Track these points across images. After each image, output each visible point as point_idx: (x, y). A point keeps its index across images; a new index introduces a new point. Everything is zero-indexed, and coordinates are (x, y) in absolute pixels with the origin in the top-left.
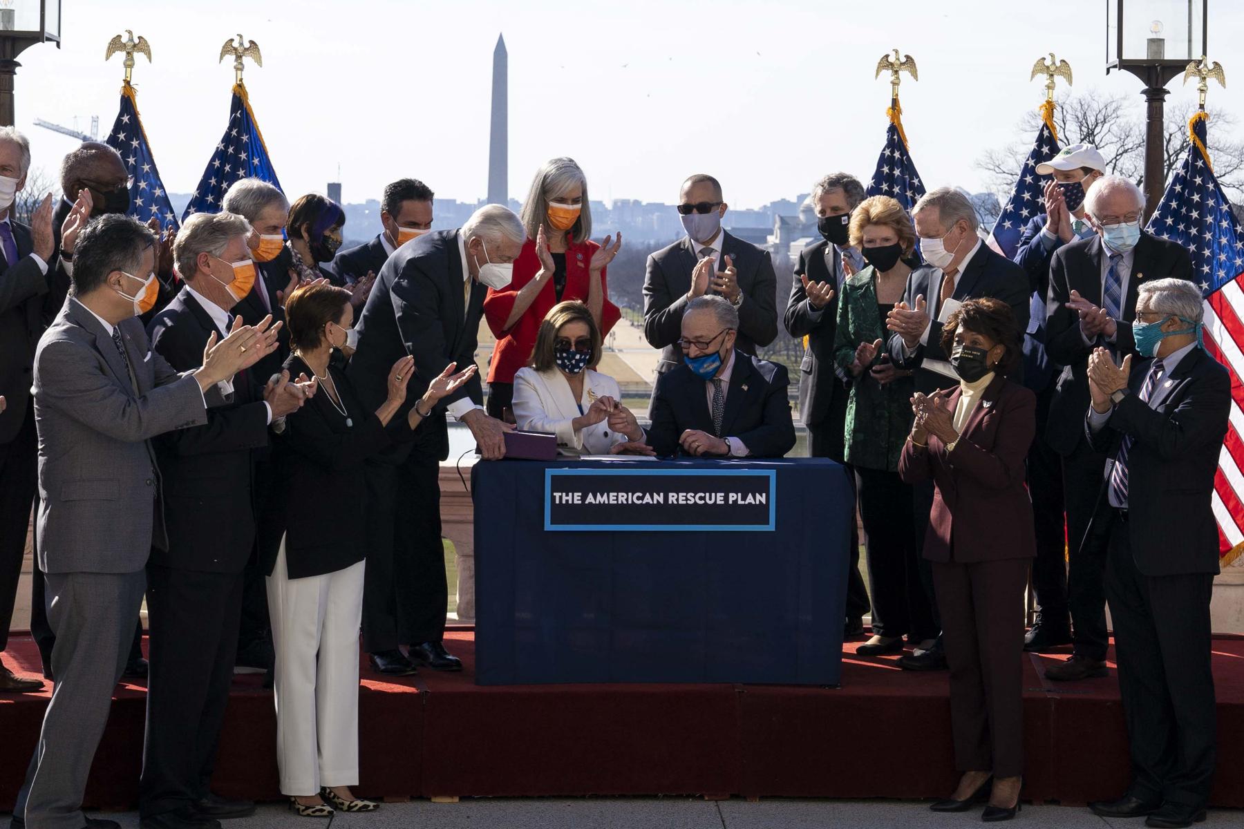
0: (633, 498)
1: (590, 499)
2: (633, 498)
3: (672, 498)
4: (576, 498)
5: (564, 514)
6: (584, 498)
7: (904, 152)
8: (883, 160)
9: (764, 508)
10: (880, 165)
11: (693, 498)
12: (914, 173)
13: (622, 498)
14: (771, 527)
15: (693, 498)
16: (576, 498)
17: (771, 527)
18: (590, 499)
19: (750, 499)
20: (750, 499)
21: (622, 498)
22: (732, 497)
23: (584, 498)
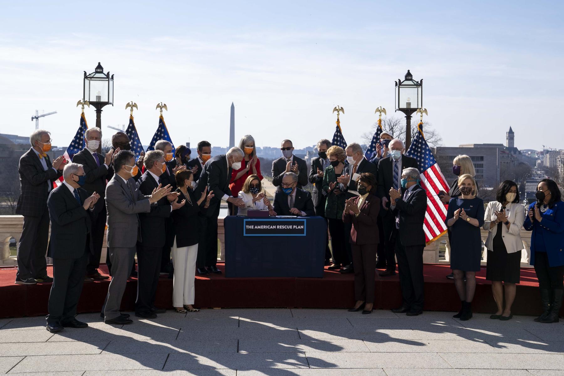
0: (268, 227)
1: (256, 227)
2: (268, 227)
3: (278, 227)
4: (252, 227)
5: (249, 231)
6: (254, 227)
7: (341, 133)
8: (335, 136)
9: (303, 230)
10: (334, 137)
11: (284, 227)
12: (343, 139)
13: (265, 227)
14: (305, 235)
15: (284, 227)
16: (252, 227)
17: (305, 235)
18: (256, 227)
19: (299, 227)
20: (299, 227)
21: (265, 227)
22: (294, 227)
23: (254, 227)
